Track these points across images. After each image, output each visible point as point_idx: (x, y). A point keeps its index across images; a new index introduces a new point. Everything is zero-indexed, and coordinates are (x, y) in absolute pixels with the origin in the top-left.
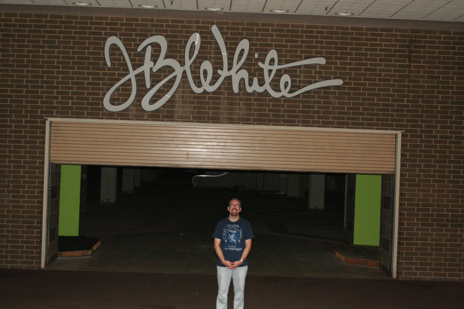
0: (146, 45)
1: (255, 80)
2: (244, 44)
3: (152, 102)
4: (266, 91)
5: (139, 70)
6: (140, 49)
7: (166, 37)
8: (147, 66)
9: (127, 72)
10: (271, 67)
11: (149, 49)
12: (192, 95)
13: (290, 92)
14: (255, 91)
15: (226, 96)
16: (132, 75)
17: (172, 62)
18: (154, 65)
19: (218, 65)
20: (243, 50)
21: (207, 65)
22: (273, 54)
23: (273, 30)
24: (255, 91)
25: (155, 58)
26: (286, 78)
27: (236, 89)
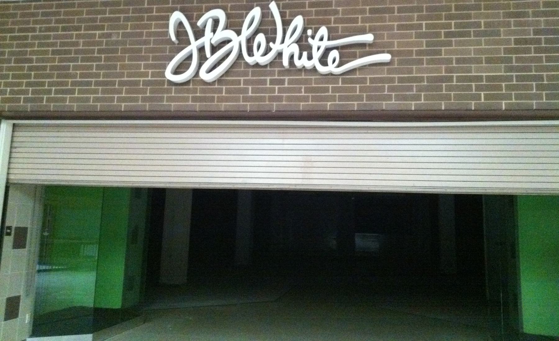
1: (305, 54)
5: (200, 41)
17: (230, 34)
19: (271, 39)
21: (261, 38)
22: (323, 31)
25: (214, 31)
26: (334, 54)
27: (285, 62)
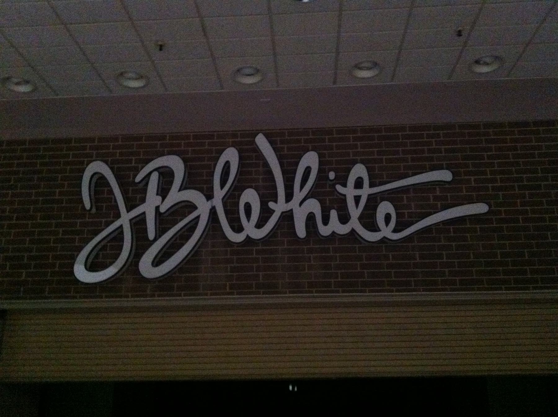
0: (148, 172)
1: (334, 214)
2: (310, 160)
3: (157, 262)
4: (353, 231)
6: (138, 179)
7: (185, 161)
8: (151, 204)
9: (118, 216)
10: (358, 192)
11: (155, 177)
12: (229, 249)
13: (395, 231)
14: (333, 232)
15: (286, 247)
16: (125, 220)
18: (163, 199)
19: (268, 195)
20: (308, 171)
21: (250, 196)
22: (359, 171)
23: (355, 139)
24: (333, 232)
25: (163, 192)
26: (385, 208)
27: (301, 231)
